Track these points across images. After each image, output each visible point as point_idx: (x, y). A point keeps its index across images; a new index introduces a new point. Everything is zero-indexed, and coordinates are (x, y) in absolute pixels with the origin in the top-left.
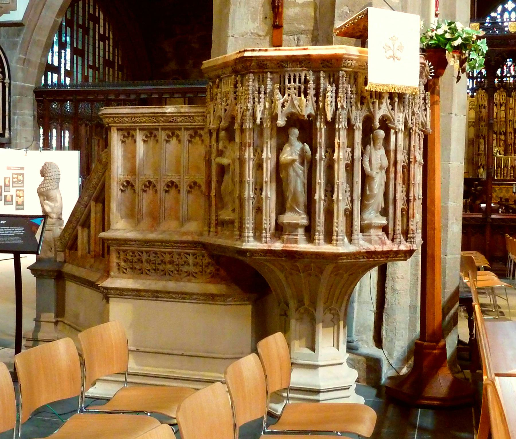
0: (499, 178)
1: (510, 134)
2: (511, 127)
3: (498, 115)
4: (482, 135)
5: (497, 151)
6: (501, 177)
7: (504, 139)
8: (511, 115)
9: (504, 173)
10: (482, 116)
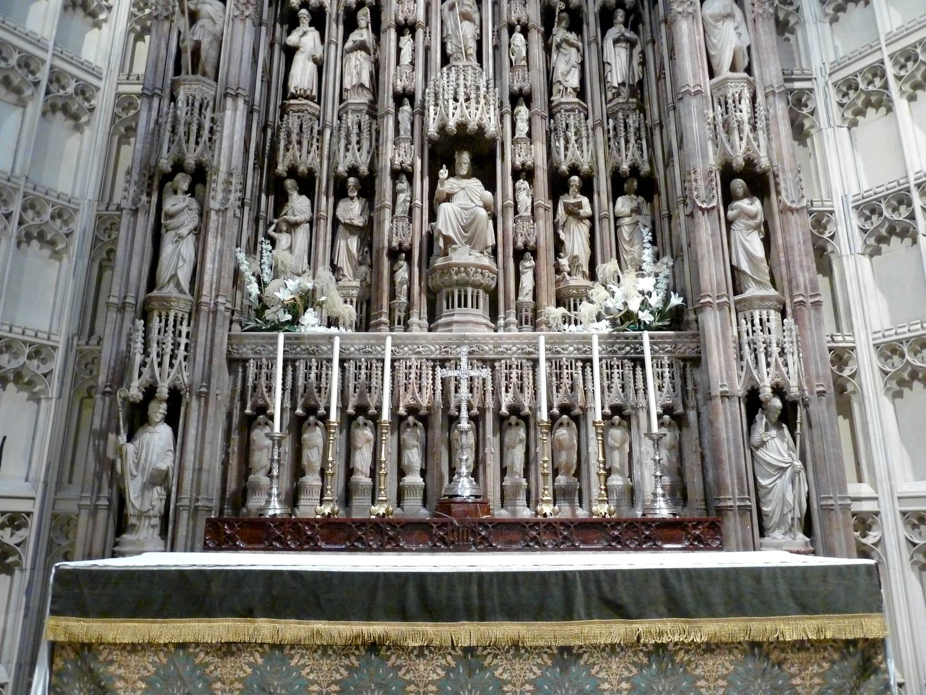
3: (331, 77)
9: (350, 471)
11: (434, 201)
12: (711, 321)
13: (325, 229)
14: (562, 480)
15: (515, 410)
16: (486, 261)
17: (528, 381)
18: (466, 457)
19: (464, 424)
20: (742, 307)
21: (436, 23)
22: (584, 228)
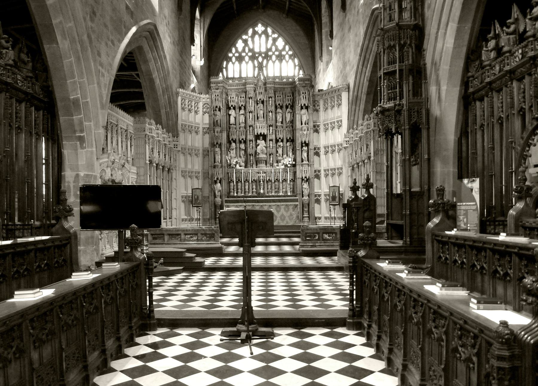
0: (239, 194)
1: (251, 142)
2: (251, 133)
3: (237, 120)
4: (217, 143)
5: (237, 162)
6: (241, 193)
7: (244, 148)
8: (251, 119)
10: (217, 121)
11: (257, 146)
12: (298, 167)
13: (238, 149)
14: (276, 190)
15: (269, 180)
16: (265, 156)
17: (271, 176)
18: (262, 187)
19: (262, 182)
20: (302, 165)
21: (256, 111)
22: (281, 149)
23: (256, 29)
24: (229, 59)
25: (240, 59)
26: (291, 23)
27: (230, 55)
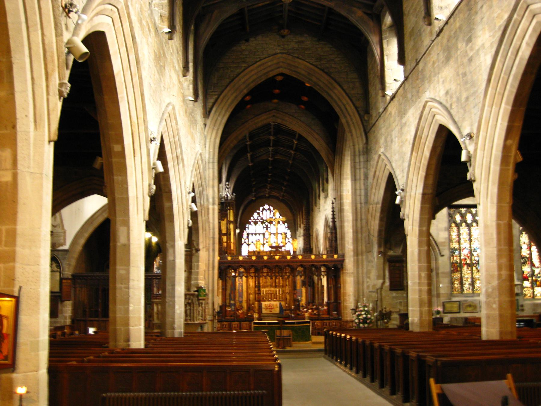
23: (264, 207)
24: (250, 223)
25: (256, 223)
26: (282, 205)
27: (250, 221)
